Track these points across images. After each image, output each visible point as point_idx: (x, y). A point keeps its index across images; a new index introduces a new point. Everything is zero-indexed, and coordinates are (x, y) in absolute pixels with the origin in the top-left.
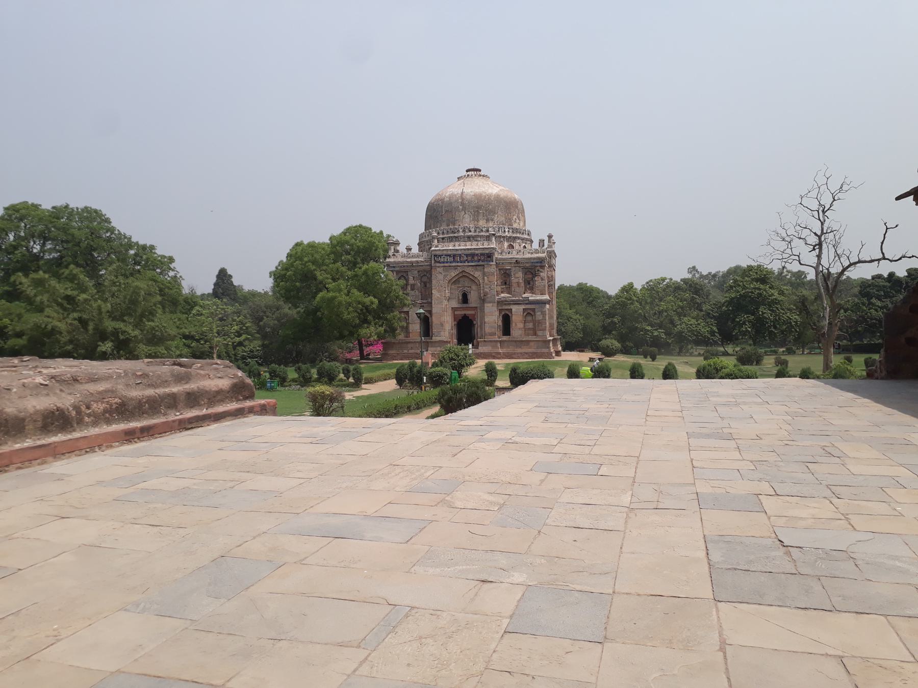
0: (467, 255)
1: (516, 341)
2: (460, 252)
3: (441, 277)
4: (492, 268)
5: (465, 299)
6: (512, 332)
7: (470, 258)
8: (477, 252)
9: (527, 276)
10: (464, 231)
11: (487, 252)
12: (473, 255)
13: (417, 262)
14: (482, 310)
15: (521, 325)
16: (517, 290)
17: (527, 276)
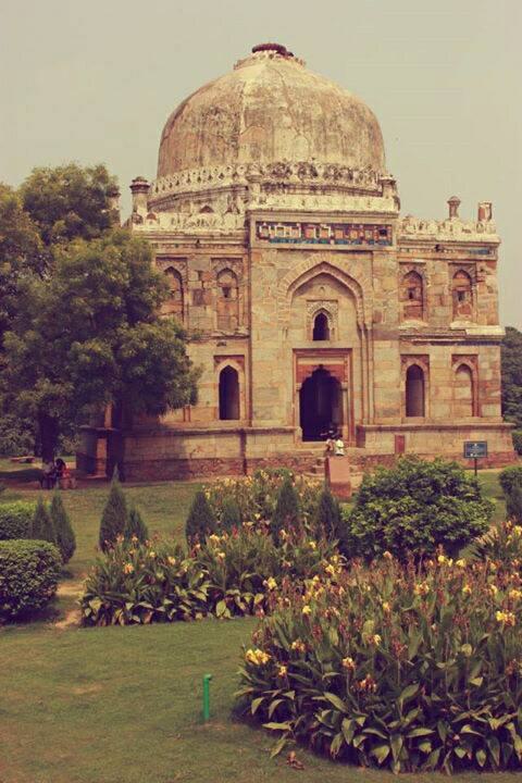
0: (333, 226)
1: (441, 429)
2: (318, 220)
3: (271, 275)
4: (388, 260)
5: (320, 328)
6: (427, 408)
7: (339, 234)
8: (356, 221)
9: (457, 282)
10: (302, 173)
11: (379, 222)
12: (347, 228)
13: (212, 237)
14: (367, 357)
15: (446, 392)
16: (440, 311)
17: (457, 282)
